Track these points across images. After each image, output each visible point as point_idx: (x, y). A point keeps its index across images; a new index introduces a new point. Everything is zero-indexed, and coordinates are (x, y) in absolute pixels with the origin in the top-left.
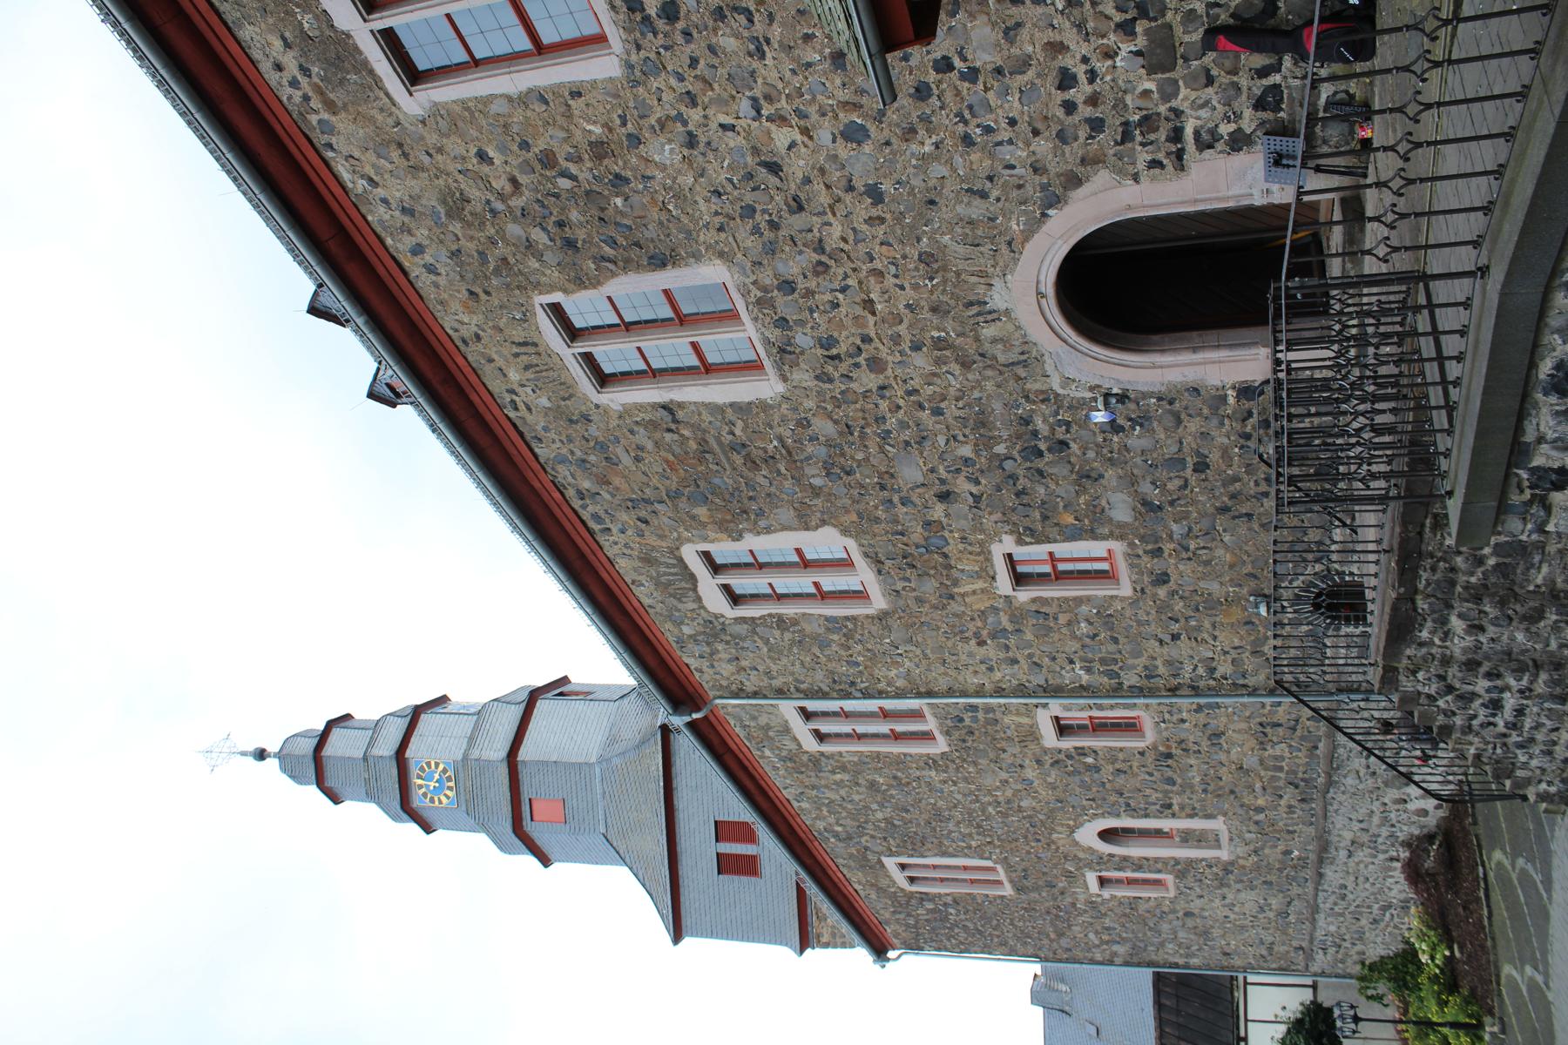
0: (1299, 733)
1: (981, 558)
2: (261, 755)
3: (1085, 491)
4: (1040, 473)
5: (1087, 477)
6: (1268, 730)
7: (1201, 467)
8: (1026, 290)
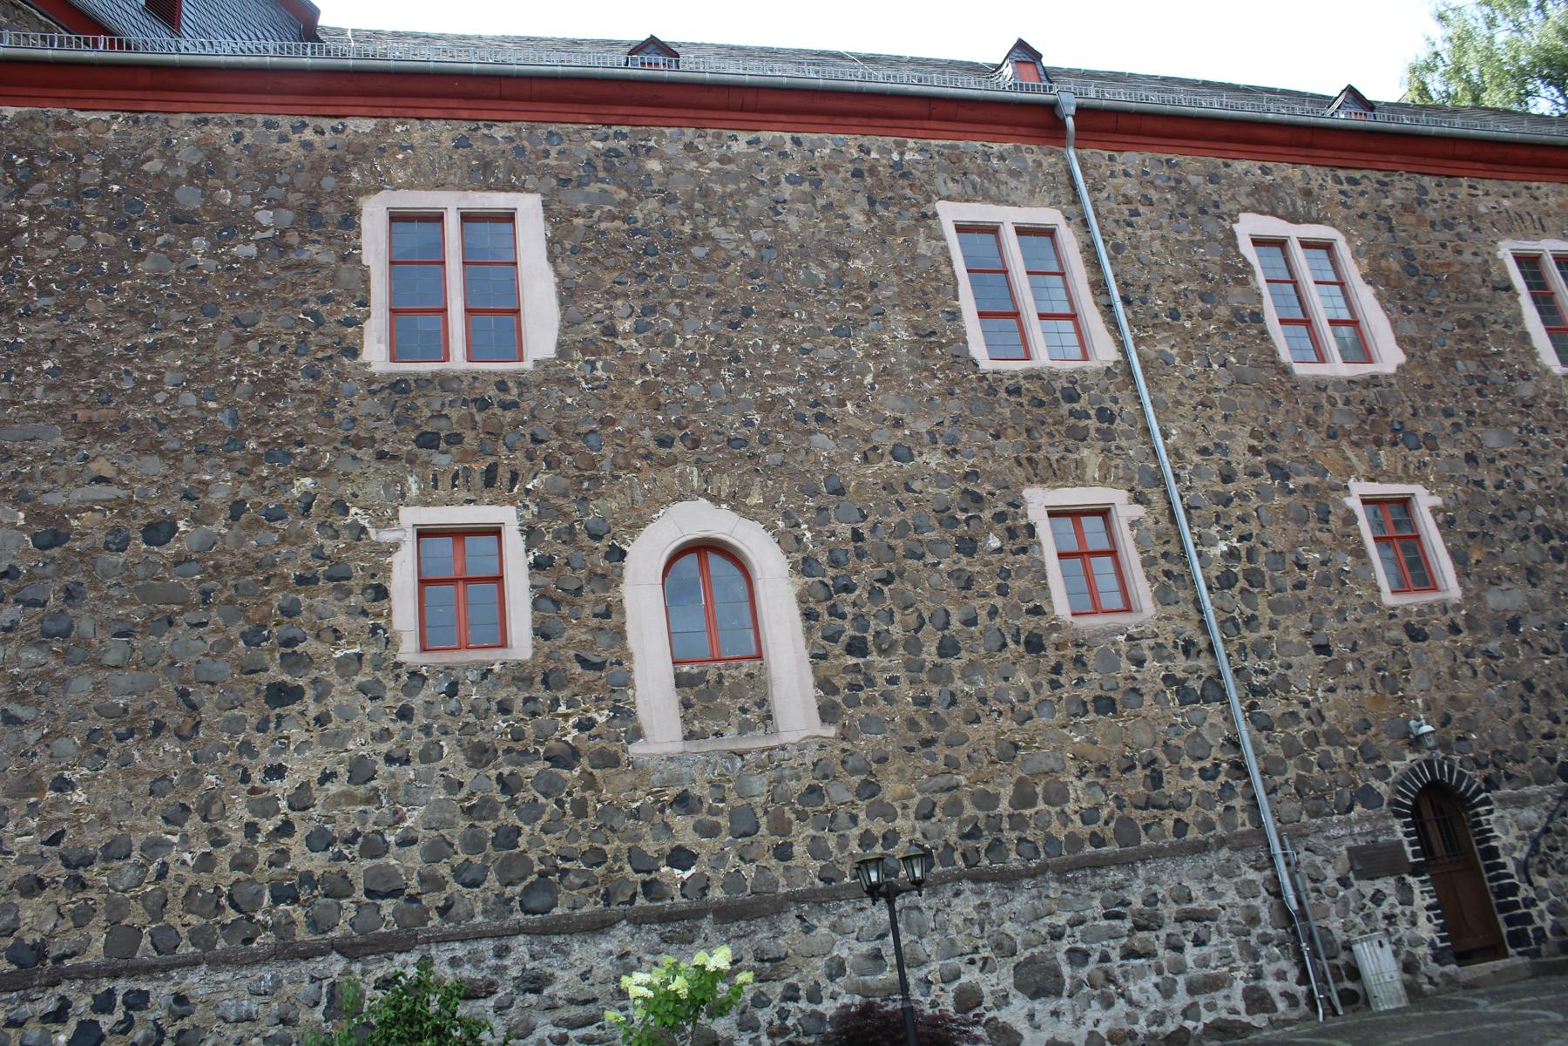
0: (1135, 814)
3: (1515, 570)
4: (1526, 538)
5: (1532, 575)
6: (1140, 773)
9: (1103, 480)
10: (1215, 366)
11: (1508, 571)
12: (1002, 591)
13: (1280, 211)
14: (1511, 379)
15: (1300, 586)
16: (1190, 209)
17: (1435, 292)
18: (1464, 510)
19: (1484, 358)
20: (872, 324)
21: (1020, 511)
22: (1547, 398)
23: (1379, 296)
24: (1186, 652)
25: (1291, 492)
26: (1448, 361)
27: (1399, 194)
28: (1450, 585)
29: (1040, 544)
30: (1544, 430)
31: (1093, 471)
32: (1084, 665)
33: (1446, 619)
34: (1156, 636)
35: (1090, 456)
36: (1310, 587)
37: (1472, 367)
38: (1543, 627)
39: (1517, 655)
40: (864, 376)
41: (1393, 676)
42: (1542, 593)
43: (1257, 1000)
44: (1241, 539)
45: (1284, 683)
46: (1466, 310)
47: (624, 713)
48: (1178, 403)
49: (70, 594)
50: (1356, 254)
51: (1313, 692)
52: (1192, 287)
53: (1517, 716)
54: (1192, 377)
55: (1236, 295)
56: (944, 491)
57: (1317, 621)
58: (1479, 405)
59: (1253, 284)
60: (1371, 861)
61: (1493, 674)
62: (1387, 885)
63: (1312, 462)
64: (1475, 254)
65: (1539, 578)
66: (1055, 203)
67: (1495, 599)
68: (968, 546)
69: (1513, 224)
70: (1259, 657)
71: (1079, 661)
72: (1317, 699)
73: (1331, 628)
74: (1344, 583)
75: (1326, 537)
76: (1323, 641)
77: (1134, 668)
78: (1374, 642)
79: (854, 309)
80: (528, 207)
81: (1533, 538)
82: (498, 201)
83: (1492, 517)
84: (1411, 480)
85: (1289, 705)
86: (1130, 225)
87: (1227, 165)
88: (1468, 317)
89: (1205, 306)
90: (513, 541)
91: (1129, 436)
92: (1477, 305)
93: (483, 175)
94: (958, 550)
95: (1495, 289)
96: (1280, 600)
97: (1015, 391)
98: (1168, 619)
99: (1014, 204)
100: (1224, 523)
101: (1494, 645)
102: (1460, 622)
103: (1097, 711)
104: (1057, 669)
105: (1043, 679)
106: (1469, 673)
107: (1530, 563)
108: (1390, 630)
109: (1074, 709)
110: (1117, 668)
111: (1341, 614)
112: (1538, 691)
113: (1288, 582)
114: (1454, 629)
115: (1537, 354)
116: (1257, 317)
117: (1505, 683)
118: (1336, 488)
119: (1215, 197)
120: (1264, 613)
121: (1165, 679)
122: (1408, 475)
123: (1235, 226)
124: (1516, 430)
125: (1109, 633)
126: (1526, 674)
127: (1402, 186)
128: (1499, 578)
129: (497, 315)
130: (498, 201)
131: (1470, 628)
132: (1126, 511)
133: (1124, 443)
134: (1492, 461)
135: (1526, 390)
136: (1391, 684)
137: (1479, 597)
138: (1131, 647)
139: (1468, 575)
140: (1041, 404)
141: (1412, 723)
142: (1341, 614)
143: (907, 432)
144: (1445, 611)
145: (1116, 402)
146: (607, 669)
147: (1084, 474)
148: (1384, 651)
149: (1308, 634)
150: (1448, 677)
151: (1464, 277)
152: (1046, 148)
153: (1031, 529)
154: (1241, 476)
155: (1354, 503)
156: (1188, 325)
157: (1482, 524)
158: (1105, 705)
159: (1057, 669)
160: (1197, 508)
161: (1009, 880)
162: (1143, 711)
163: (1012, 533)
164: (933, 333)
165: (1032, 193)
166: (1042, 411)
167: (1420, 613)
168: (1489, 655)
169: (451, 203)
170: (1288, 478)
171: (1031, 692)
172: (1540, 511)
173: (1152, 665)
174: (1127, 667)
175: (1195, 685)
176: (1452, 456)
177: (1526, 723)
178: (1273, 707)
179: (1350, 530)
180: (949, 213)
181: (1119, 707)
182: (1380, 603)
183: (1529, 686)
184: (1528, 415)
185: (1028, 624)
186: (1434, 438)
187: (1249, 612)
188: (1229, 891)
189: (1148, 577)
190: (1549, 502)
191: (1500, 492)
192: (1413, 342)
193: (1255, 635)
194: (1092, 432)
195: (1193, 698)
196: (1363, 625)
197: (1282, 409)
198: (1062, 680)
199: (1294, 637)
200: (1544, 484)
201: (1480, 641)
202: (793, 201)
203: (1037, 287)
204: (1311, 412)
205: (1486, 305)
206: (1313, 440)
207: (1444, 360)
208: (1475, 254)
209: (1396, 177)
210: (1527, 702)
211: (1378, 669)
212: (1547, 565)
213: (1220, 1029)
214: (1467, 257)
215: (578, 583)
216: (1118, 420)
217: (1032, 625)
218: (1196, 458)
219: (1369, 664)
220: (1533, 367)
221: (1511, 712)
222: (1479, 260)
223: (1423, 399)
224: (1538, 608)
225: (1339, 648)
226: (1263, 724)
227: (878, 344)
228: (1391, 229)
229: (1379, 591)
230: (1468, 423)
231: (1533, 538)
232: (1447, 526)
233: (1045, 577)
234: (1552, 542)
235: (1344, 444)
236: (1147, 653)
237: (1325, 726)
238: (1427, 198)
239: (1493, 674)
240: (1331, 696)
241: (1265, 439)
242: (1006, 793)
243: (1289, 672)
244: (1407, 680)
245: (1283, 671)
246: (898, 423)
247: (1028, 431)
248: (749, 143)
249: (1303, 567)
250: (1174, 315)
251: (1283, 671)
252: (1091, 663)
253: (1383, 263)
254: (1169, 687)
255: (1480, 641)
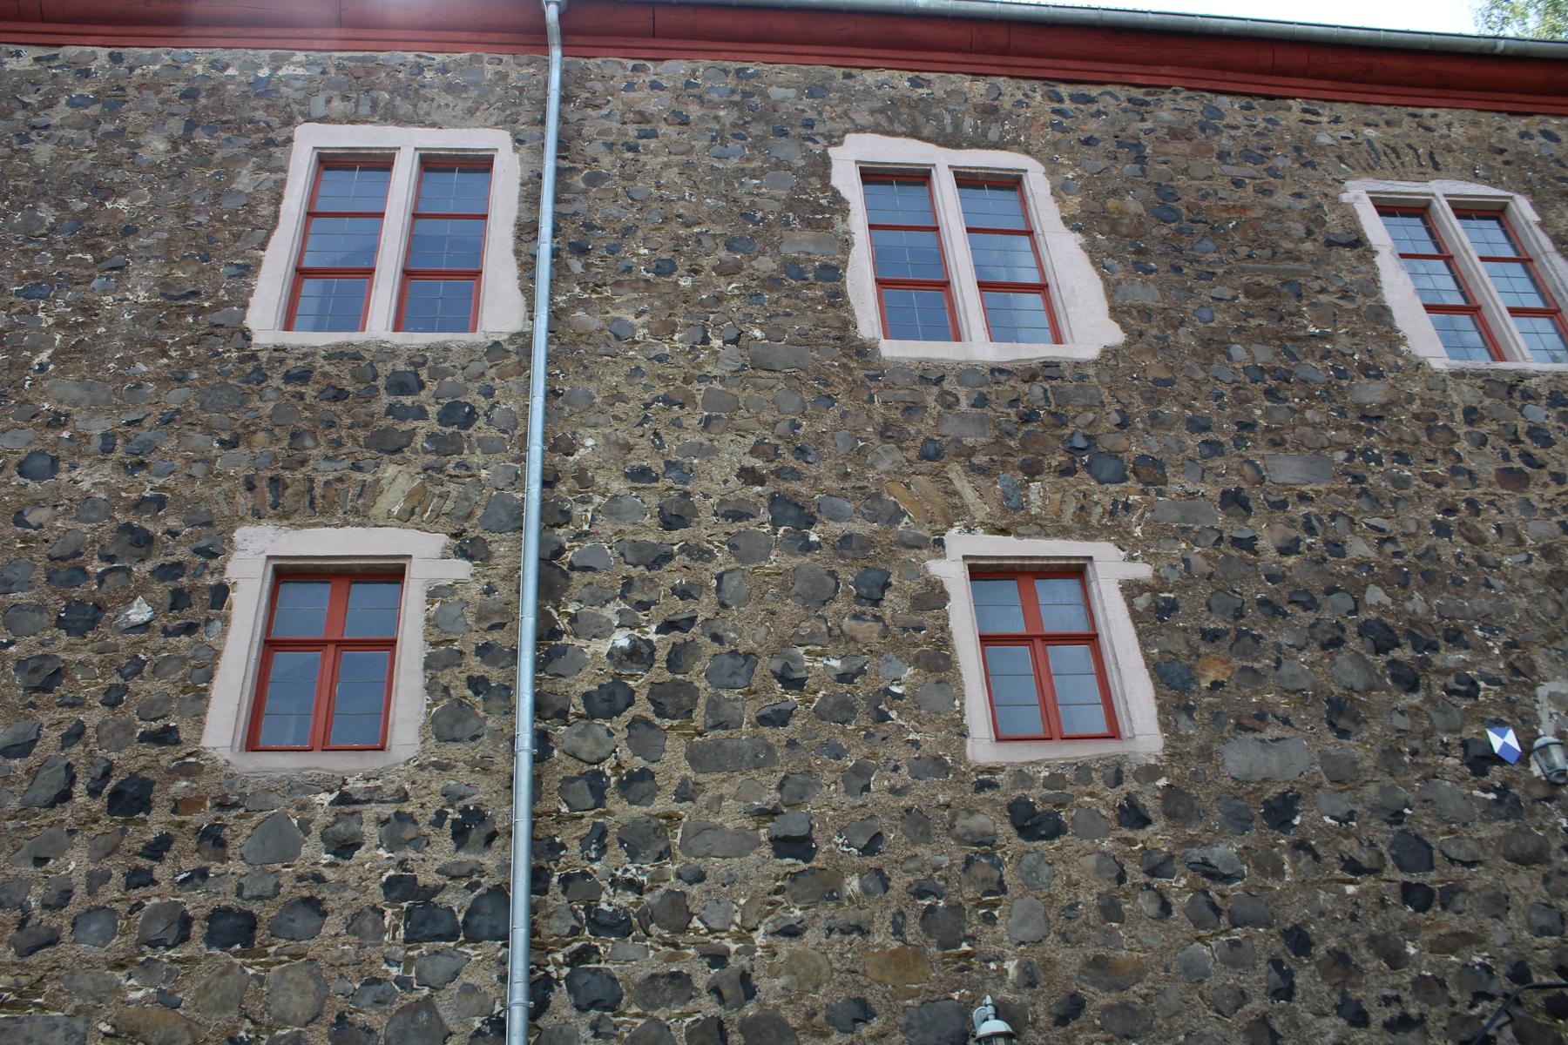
1: (1067, 519)
5: (1341, 714)
7: (1419, 897)
9: (406, 518)
10: (716, 343)
11: (1284, 705)
12: (113, 698)
13: (926, 132)
14: (1341, 375)
15: (779, 718)
16: (756, 129)
17: (1208, 244)
18: (1203, 590)
19: (1291, 342)
20: (95, 283)
21: (213, 563)
22: (1415, 407)
23: (1092, 250)
24: (460, 835)
25: (809, 547)
26: (1215, 345)
27: (1166, 115)
29: (226, 620)
30: (1402, 458)
31: (392, 501)
32: (220, 843)
33: (1115, 795)
34: (405, 798)
35: (397, 481)
36: (796, 723)
37: (1264, 355)
38: (1351, 815)
39: (1278, 872)
40: (36, 350)
41: (956, 909)
42: (1360, 750)
44: (667, 627)
45: (676, 913)
46: (1267, 271)
48: (619, 397)
50: (1060, 192)
51: (745, 934)
52: (718, 230)
53: (1257, 1005)
54: (660, 358)
55: (799, 242)
56: (85, 527)
57: (796, 790)
58: (1267, 414)
59: (839, 227)
61: (1208, 914)
63: (877, 496)
64: (1298, 195)
65: (1357, 721)
66: (508, 122)
67: (1240, 758)
68: (83, 619)
70: (633, 855)
71: (213, 839)
72: (749, 951)
73: (828, 802)
74: (883, 717)
75: (867, 631)
76: (797, 830)
77: (327, 858)
78: (926, 836)
79: (80, 263)
81: (1353, 643)
83: (1263, 603)
84: (1088, 534)
85: (671, 958)
86: (633, 148)
87: (848, 76)
88: (1269, 281)
91: (488, 447)
92: (1291, 265)
94: (60, 623)
95: (1330, 244)
96: (718, 744)
97: (303, 376)
98: (442, 767)
99: (433, 125)
100: (637, 596)
101: (1224, 852)
102: (1150, 802)
103: (210, 940)
104: (157, 849)
105: (117, 869)
106: (1152, 908)
107: (1337, 691)
108: (971, 813)
109: (157, 930)
110: (288, 853)
111: (858, 780)
112: (1320, 951)
113: (750, 710)
114: (1133, 815)
115: (1403, 340)
116: (833, 273)
117: (1238, 933)
118: (916, 544)
119: (810, 114)
120: (674, 763)
121: (389, 885)
122: (1086, 525)
123: (832, 151)
124: (1340, 456)
125: (298, 787)
126: (1294, 914)
127: (1174, 107)
128: (1261, 717)
131: (1170, 815)
133: (477, 459)
134: (1282, 505)
135: (1372, 393)
136: (945, 927)
137: (1205, 754)
138: (338, 818)
139: (1189, 710)
140: (339, 395)
141: (976, 1014)
142: (858, 780)
143: (66, 434)
144: (1118, 779)
145: (488, 393)
147: (368, 507)
148: (945, 855)
149: (770, 814)
150: (1094, 916)
151: (1268, 226)
152: (524, 58)
153: (221, 594)
154: (706, 517)
155: (950, 571)
156: (686, 283)
157: (1239, 614)
158: (234, 929)
159: (157, 849)
160: (585, 569)
162: (313, 947)
163: (179, 600)
164: (195, 294)
165: (471, 112)
166: (338, 407)
167: (1054, 781)
168: (1207, 870)
170: (810, 524)
171: (80, 890)
172: (1375, 595)
173: (375, 857)
174: (314, 853)
175: (456, 900)
176: (1191, 495)
177: (1277, 1024)
178: (630, 961)
179: (927, 618)
181: (261, 934)
182: (960, 756)
183: (1299, 941)
184: (1370, 433)
185: (130, 759)
186: (1159, 465)
187: (638, 763)
189: (429, 689)
190: (1398, 581)
191: (1291, 560)
192: (1145, 313)
193: (638, 811)
194: (419, 440)
195: (442, 929)
196: (906, 801)
197: (835, 412)
198: (161, 871)
199: (731, 818)
200: (1389, 548)
201: (1192, 842)
202: (62, 126)
204: (896, 415)
205: (1309, 266)
206: (887, 460)
207: (1207, 343)
208: (1298, 195)
209: (1167, 96)
210: (1288, 976)
211: (921, 893)
212: (1379, 696)
214: (1282, 198)
216: (481, 422)
217: (142, 761)
218: (618, 486)
219: (899, 882)
220: (1390, 358)
221: (1242, 997)
222: (1305, 203)
223: (1147, 401)
224: (1343, 777)
225: (831, 846)
227: (88, 309)
228: (1140, 159)
229: (963, 734)
230: (1239, 442)
231: (1353, 643)
233: (209, 677)
234: (1396, 653)
235: (955, 472)
236: (371, 831)
237: (750, 1010)
238: (1220, 124)
239: (1208, 914)
240: (785, 947)
241: (779, 458)
243: (695, 890)
244: (989, 919)
245: (680, 886)
246: (57, 421)
247: (295, 436)
248: (37, 60)
249: (792, 682)
250: (664, 269)
251: (680, 886)
252: (235, 846)
253: (1112, 203)
254: (394, 902)
255: (1192, 842)
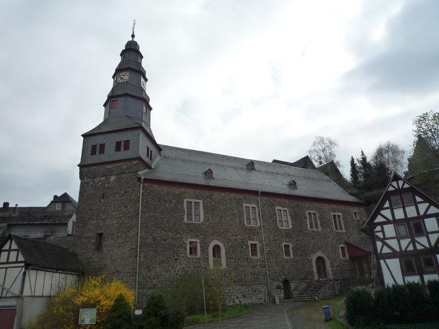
2: (133, 36)
8: (320, 254)
28: (292, 257)
43: (265, 301)
47: (208, 264)
49: (156, 247)
60: (278, 287)
62: (279, 290)
69: (309, 208)
80: (201, 202)
82: (198, 201)
89: (270, 218)
90: (198, 244)
93: (196, 197)
129: (198, 215)
130: (198, 201)
132: (258, 245)
146: (207, 259)
158: (254, 267)
161: (242, 285)
169: (193, 201)
178: (271, 269)
180: (245, 205)
188: (263, 288)
203: (252, 213)
213: (261, 304)
215: (205, 249)
226: (269, 271)
232: (293, 249)
242: (243, 276)
